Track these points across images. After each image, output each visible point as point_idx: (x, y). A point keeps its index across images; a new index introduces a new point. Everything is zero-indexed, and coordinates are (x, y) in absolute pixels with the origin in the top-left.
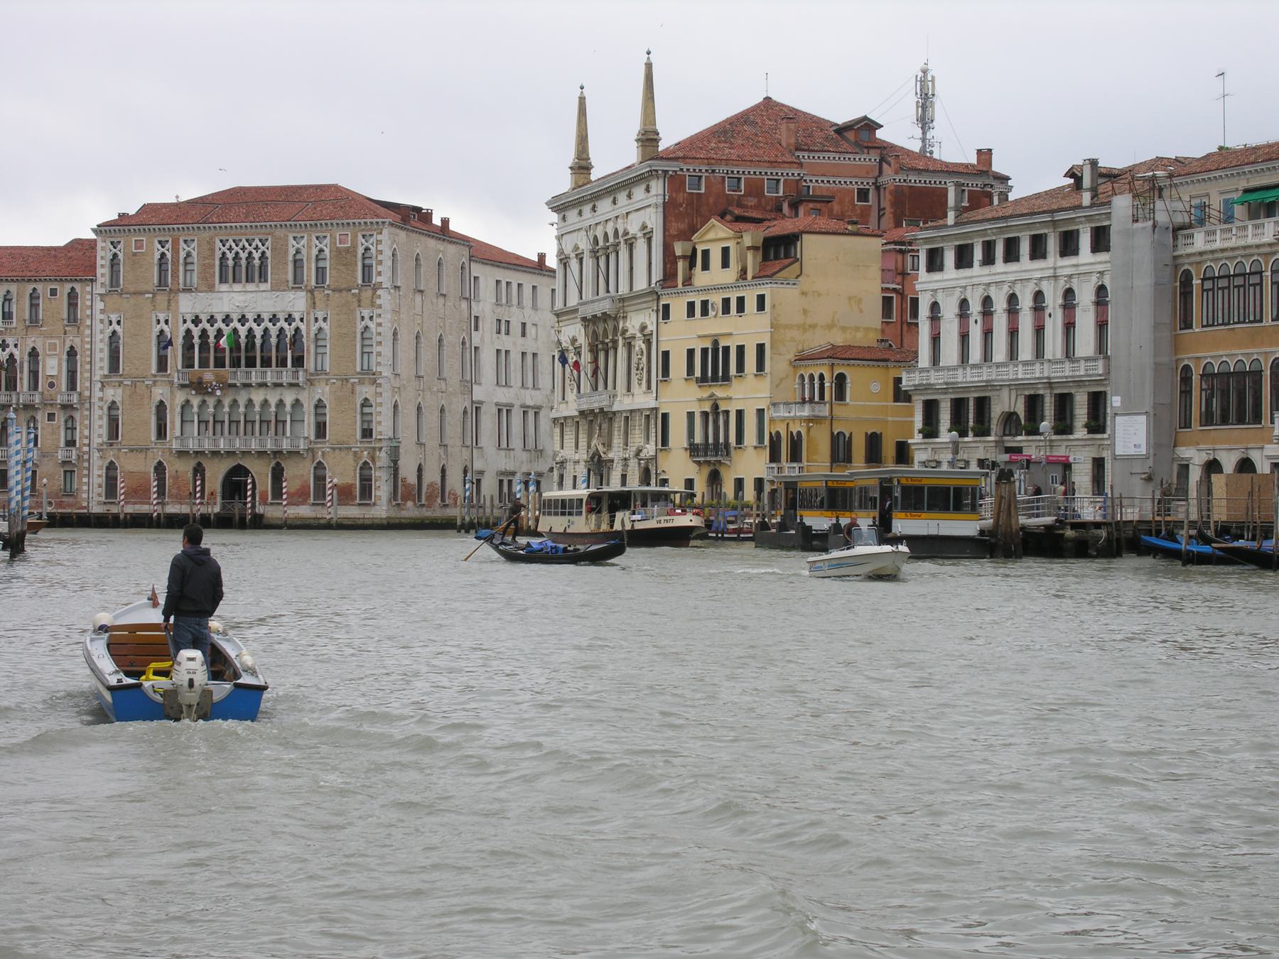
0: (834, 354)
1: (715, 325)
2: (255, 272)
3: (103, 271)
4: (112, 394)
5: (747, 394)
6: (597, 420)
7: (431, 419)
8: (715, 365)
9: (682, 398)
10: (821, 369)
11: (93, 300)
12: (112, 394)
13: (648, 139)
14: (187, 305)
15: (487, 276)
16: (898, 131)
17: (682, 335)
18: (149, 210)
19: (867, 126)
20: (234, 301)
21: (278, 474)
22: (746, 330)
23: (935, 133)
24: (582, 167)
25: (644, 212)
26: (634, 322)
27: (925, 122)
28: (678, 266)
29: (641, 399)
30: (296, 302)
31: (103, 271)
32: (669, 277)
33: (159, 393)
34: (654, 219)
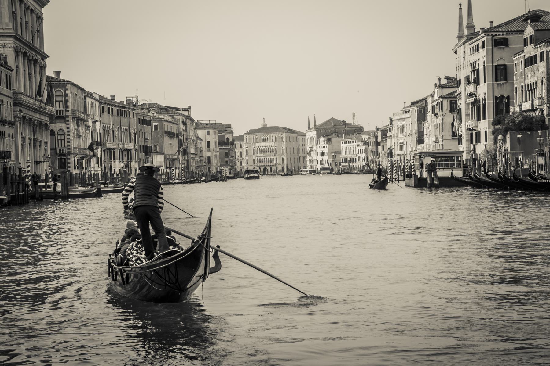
0: (335, 153)
1: (322, 149)
2: (266, 140)
3: (245, 140)
4: (247, 158)
5: (326, 157)
6: (311, 160)
7: (292, 160)
8: (322, 154)
9: (319, 158)
10: (333, 154)
11: (244, 144)
12: (247, 158)
13: (315, 125)
14: (257, 145)
15: (300, 138)
16: (349, 121)
17: (319, 150)
18: (250, 131)
19: (344, 122)
20: (263, 144)
21: (271, 168)
22: (326, 150)
23: (356, 120)
24: (309, 127)
25: (314, 134)
26: (315, 148)
27: (354, 119)
28: (318, 142)
29: (314, 158)
30: (273, 144)
31: (245, 140)
32: (317, 143)
33: (254, 157)
34: (315, 136)
